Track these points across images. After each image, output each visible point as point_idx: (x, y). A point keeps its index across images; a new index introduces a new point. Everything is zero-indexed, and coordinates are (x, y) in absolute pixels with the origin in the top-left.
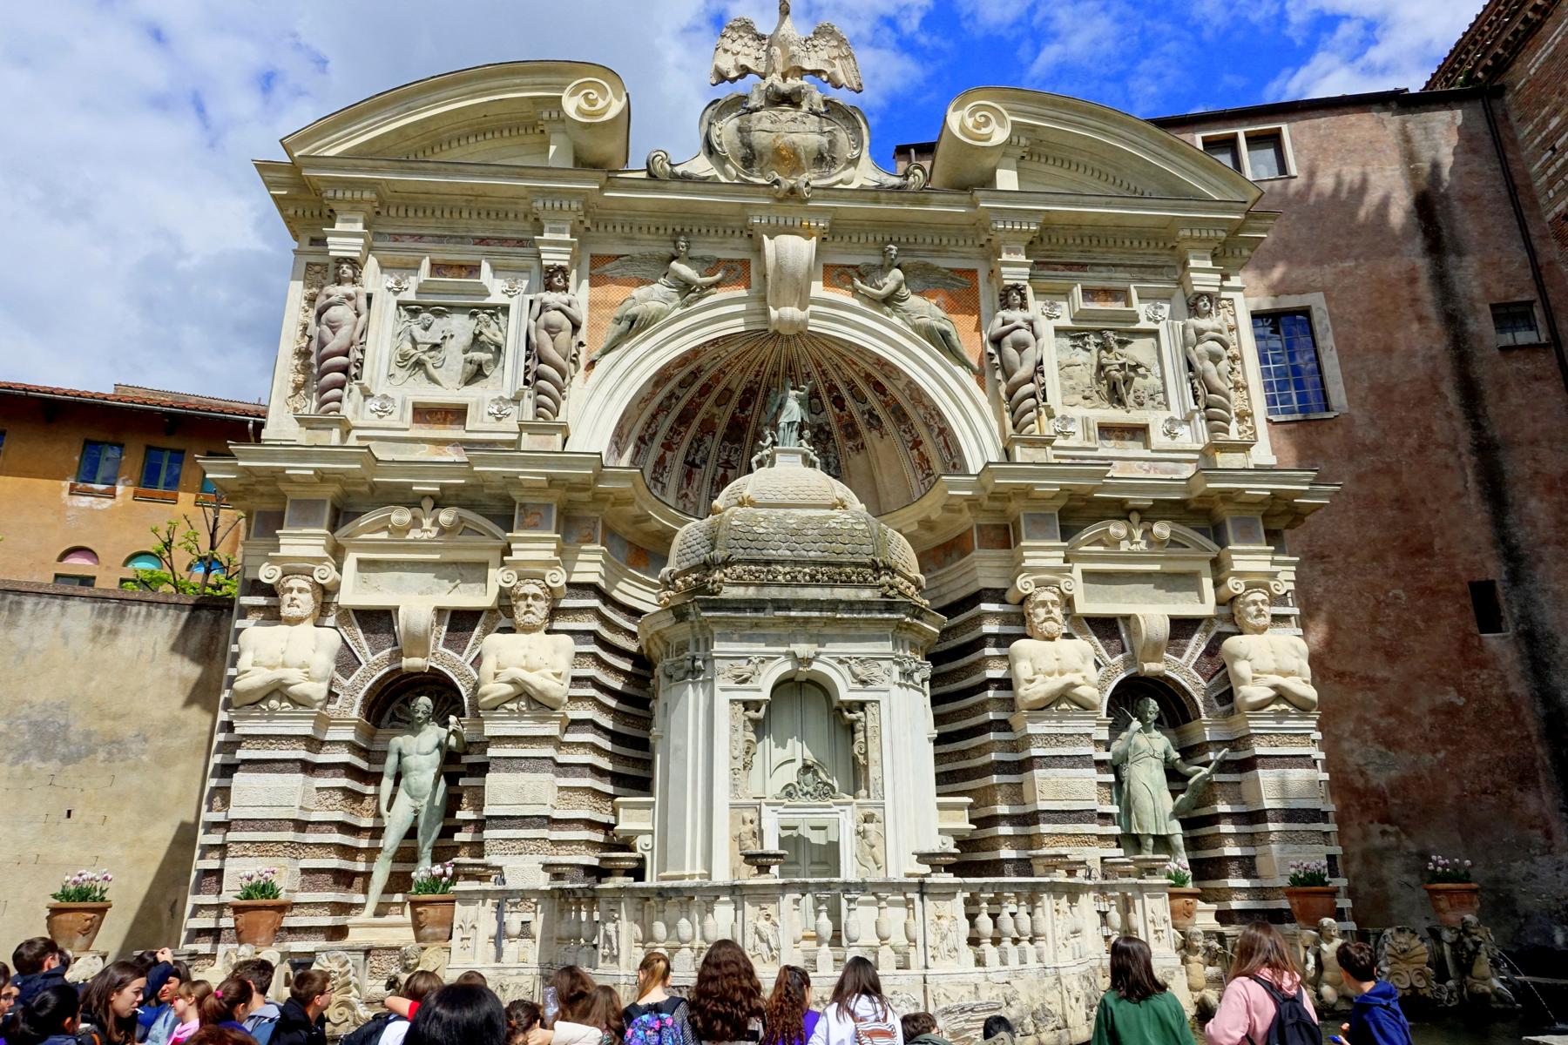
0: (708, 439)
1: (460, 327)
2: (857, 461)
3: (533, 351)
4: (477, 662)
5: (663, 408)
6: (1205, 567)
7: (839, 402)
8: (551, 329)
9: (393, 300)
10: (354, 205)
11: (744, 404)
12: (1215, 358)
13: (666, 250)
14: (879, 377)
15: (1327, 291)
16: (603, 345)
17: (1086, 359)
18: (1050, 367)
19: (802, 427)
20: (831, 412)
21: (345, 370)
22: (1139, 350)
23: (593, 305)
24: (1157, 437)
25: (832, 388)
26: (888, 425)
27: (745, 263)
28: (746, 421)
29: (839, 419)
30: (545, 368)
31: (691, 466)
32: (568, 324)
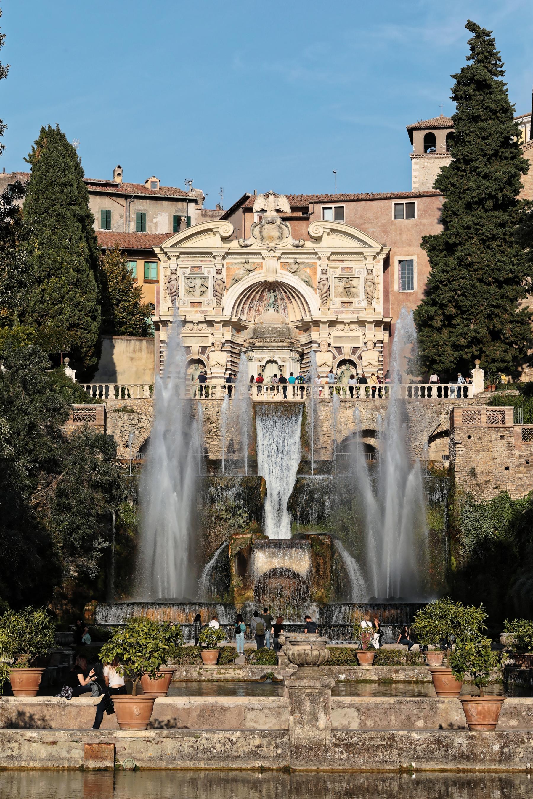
1: (198, 282)
3: (215, 290)
4: (208, 358)
7: (285, 292)
8: (219, 285)
12: (370, 287)
13: (244, 261)
14: (294, 289)
15: (418, 255)
16: (229, 286)
17: (342, 284)
18: (332, 289)
22: (354, 283)
23: (227, 275)
24: (356, 304)
30: (217, 294)
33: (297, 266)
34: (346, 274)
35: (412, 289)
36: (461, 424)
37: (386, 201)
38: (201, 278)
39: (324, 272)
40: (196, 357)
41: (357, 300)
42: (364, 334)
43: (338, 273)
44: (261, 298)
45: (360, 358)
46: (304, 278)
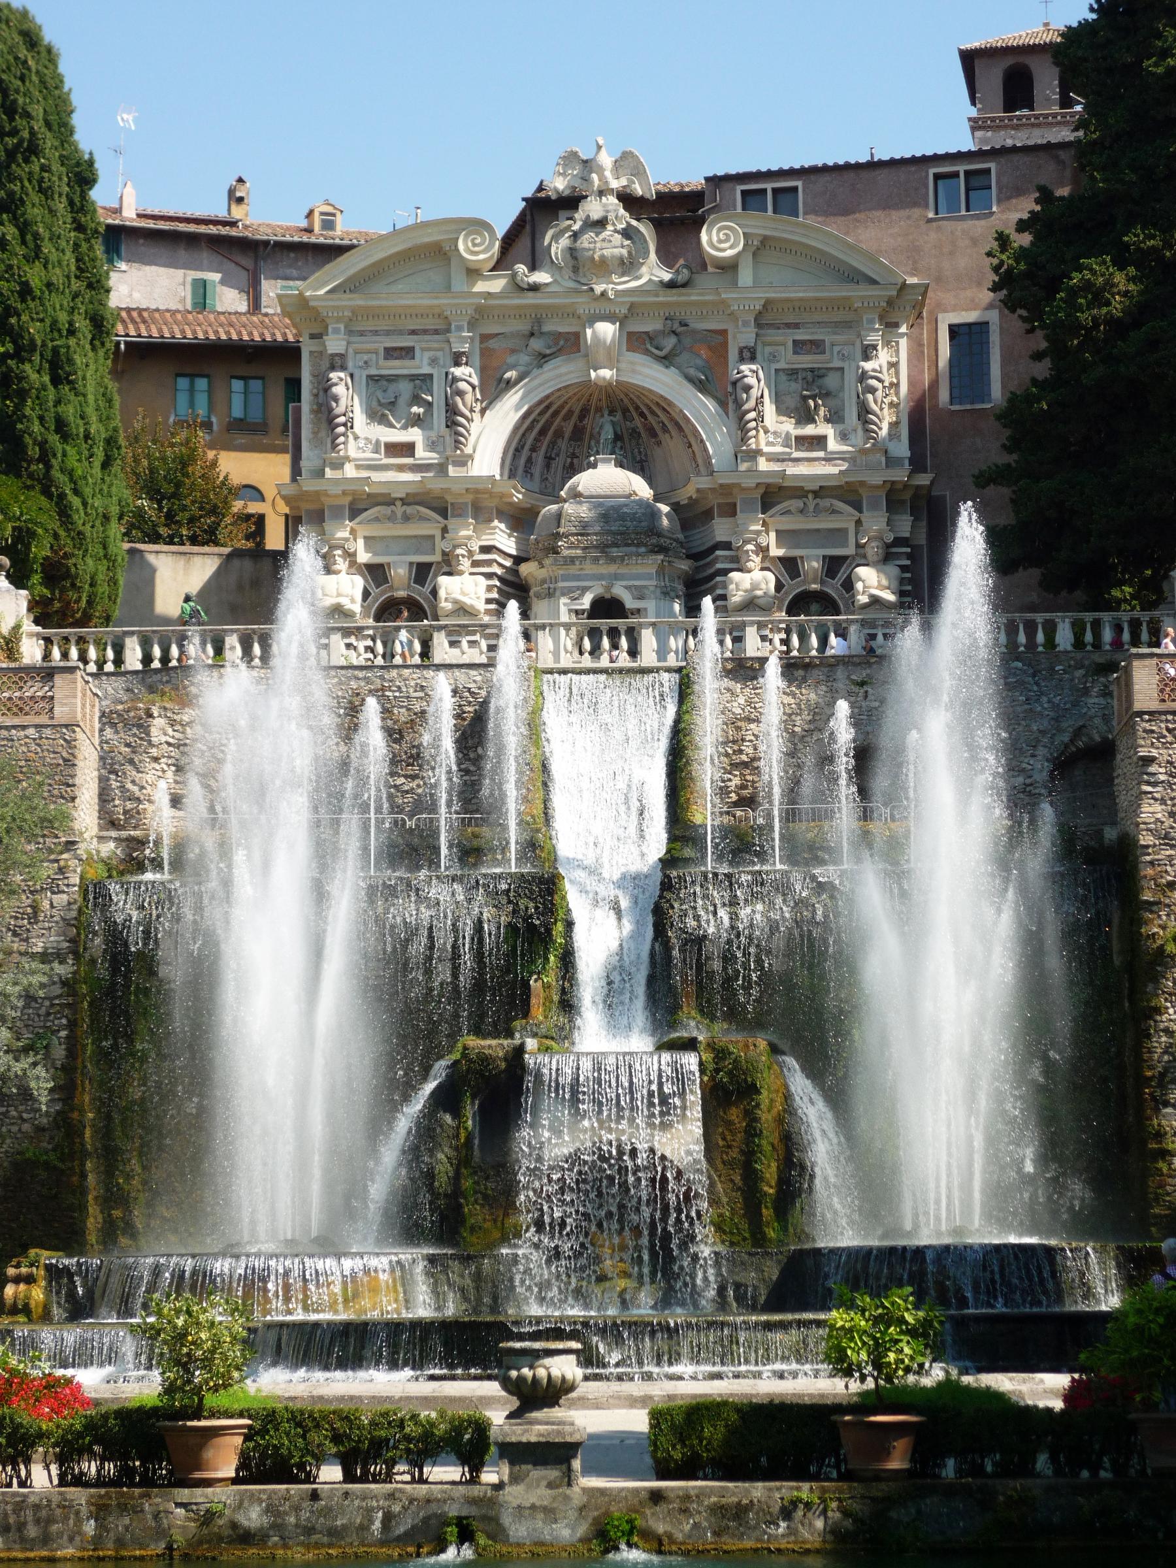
0: (559, 441)
1: (405, 388)
2: (658, 452)
4: (434, 592)
5: (530, 428)
6: (852, 527)
7: (642, 415)
9: (365, 373)
10: (338, 320)
11: (582, 417)
19: (618, 437)
20: (638, 422)
21: (345, 425)
25: (637, 408)
26: (674, 432)
28: (584, 428)
29: (645, 425)
31: (549, 459)
32: (469, 389)
33: (673, 340)
34: (806, 361)
36: (1155, 705)
38: (413, 378)
39: (746, 354)
40: (402, 594)
41: (841, 427)
42: (859, 523)
43: (787, 359)
44: (578, 434)
45: (849, 585)
46: (692, 372)
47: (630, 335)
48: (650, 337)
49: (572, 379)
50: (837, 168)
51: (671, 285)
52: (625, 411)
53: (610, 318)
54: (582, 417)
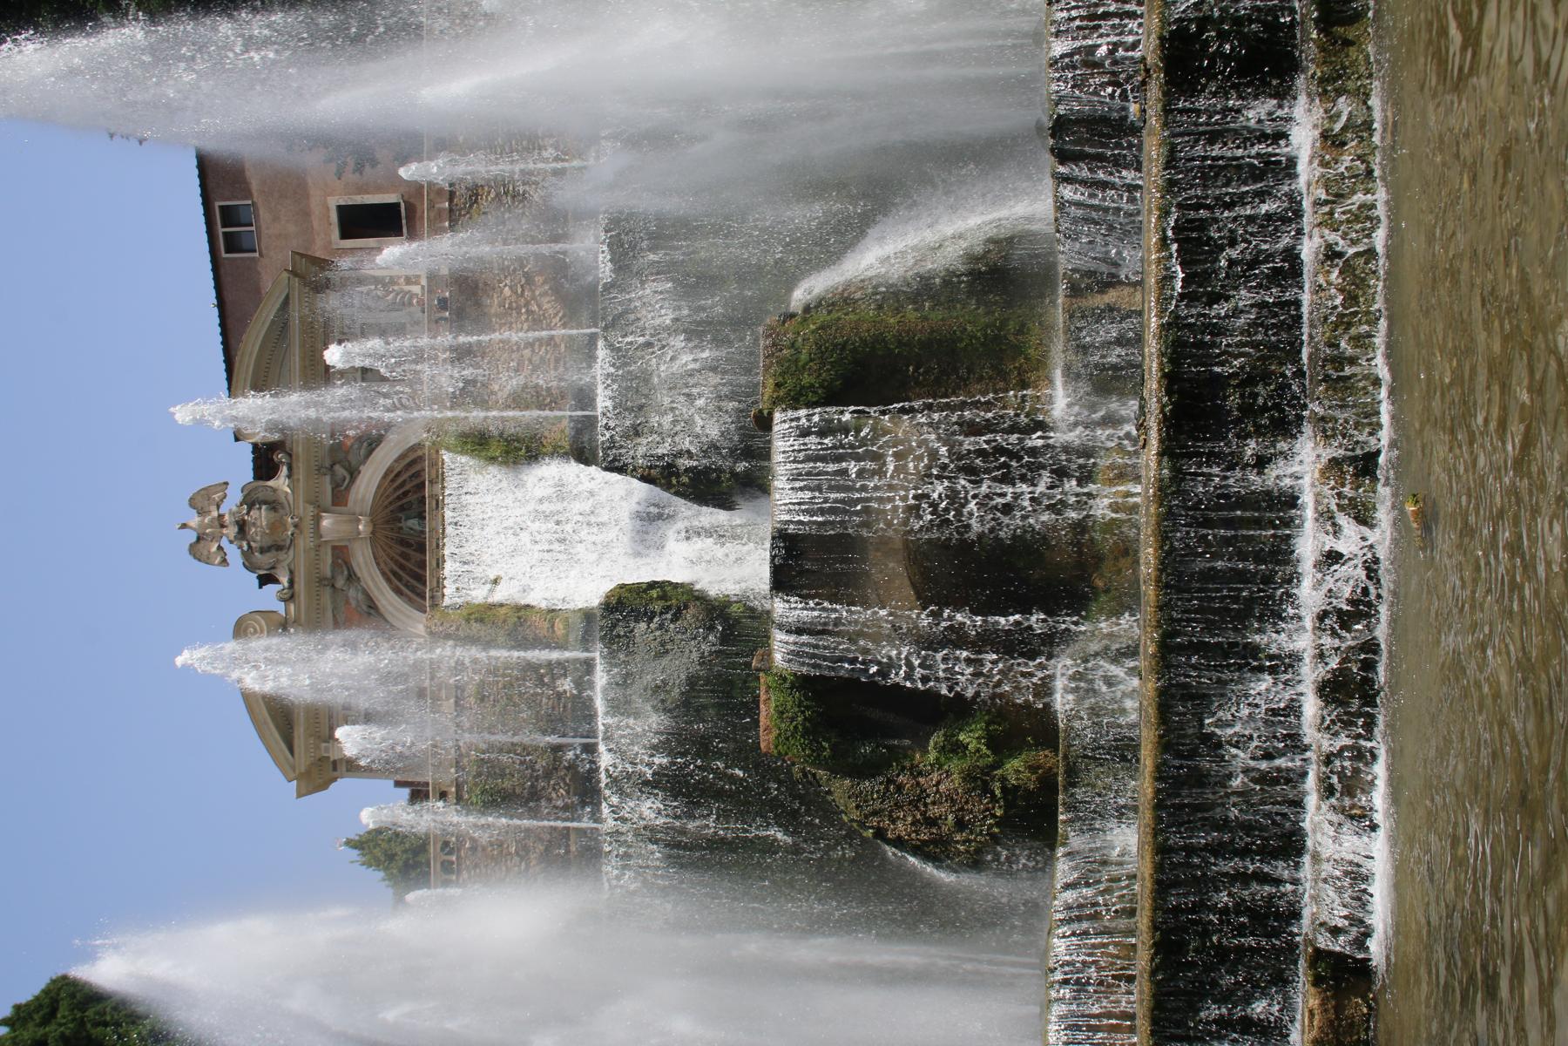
7: (405, 494)
10: (317, 748)
11: (409, 545)
14: (392, 476)
25: (399, 498)
27: (334, 548)
33: (338, 468)
35: (398, 205)
37: (222, 271)
47: (334, 504)
48: (336, 486)
49: (368, 552)
50: (224, 333)
51: (290, 469)
52: (402, 509)
53: (317, 520)
54: (409, 545)
